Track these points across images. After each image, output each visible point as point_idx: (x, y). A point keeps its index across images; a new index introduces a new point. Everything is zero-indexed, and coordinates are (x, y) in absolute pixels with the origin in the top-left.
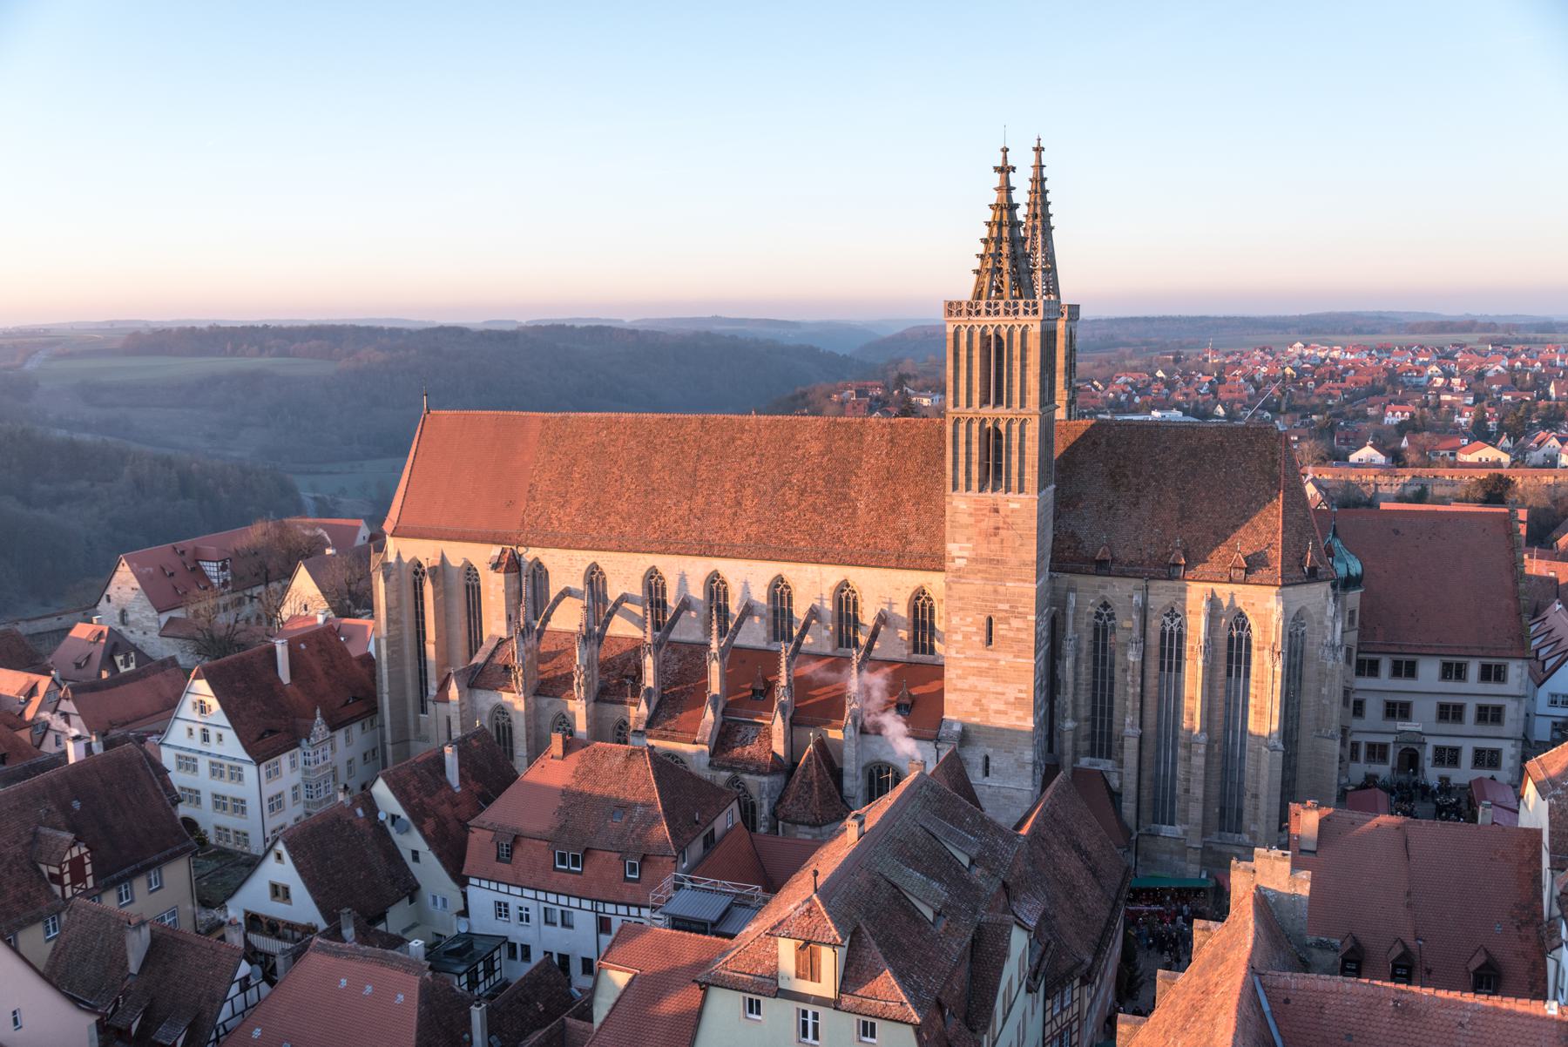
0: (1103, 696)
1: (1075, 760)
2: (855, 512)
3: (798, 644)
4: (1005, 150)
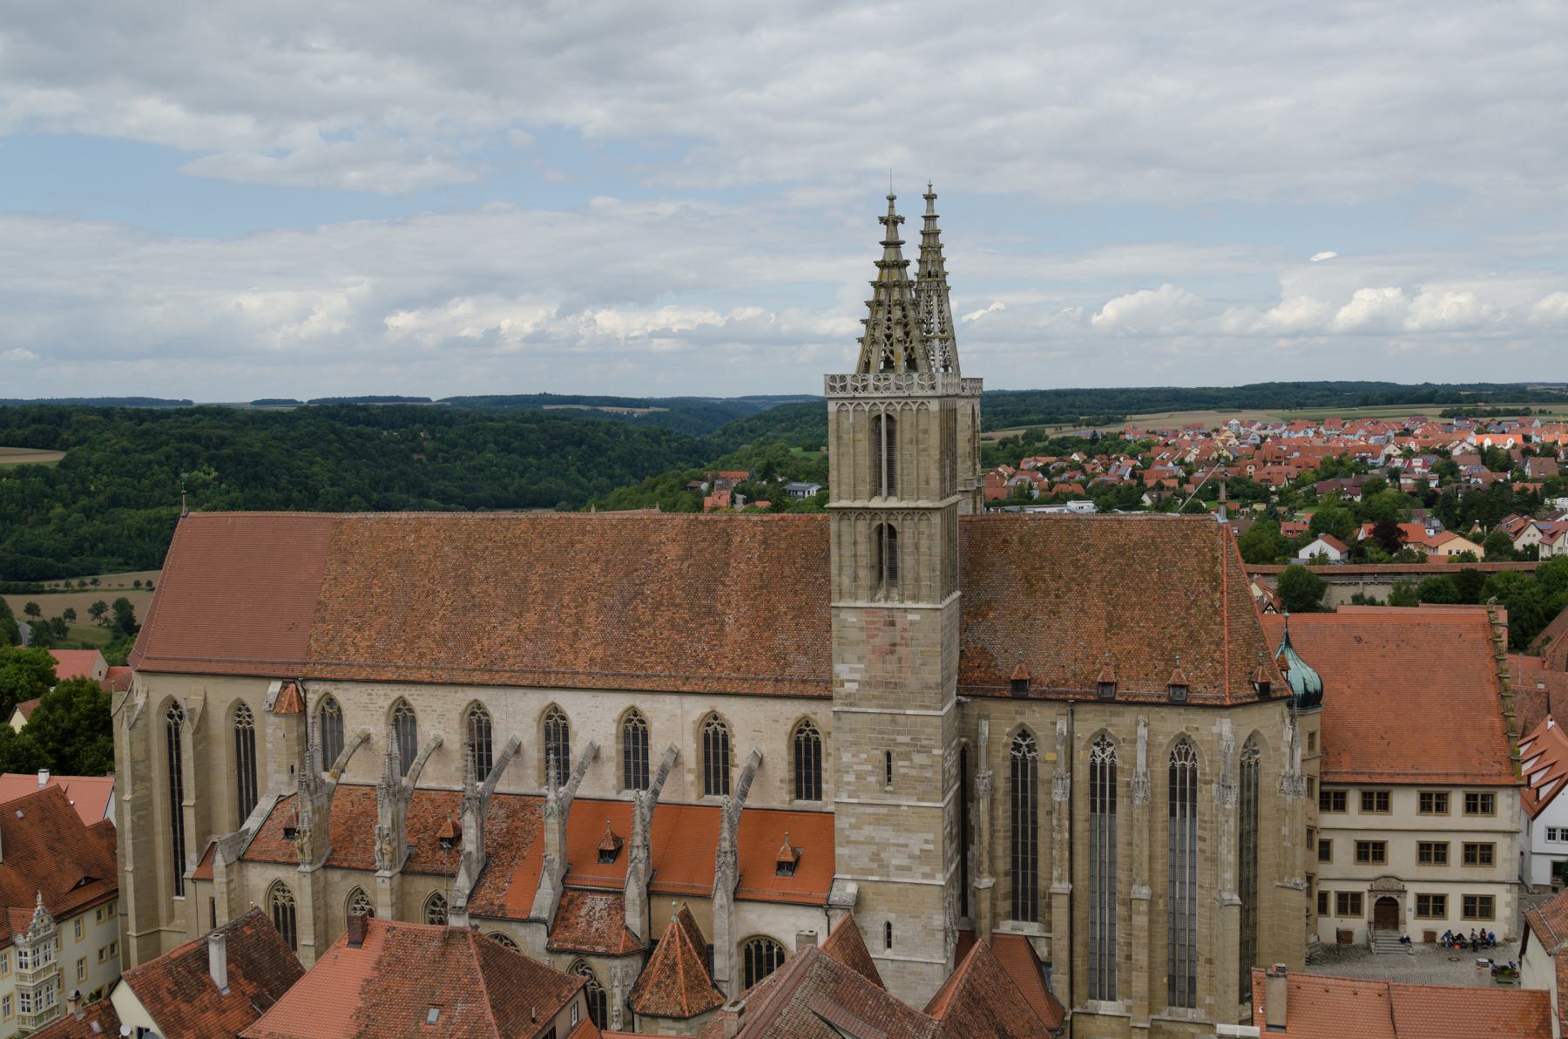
0: (1025, 845)
1: (994, 924)
2: (721, 630)
3: (656, 793)
4: (891, 199)
